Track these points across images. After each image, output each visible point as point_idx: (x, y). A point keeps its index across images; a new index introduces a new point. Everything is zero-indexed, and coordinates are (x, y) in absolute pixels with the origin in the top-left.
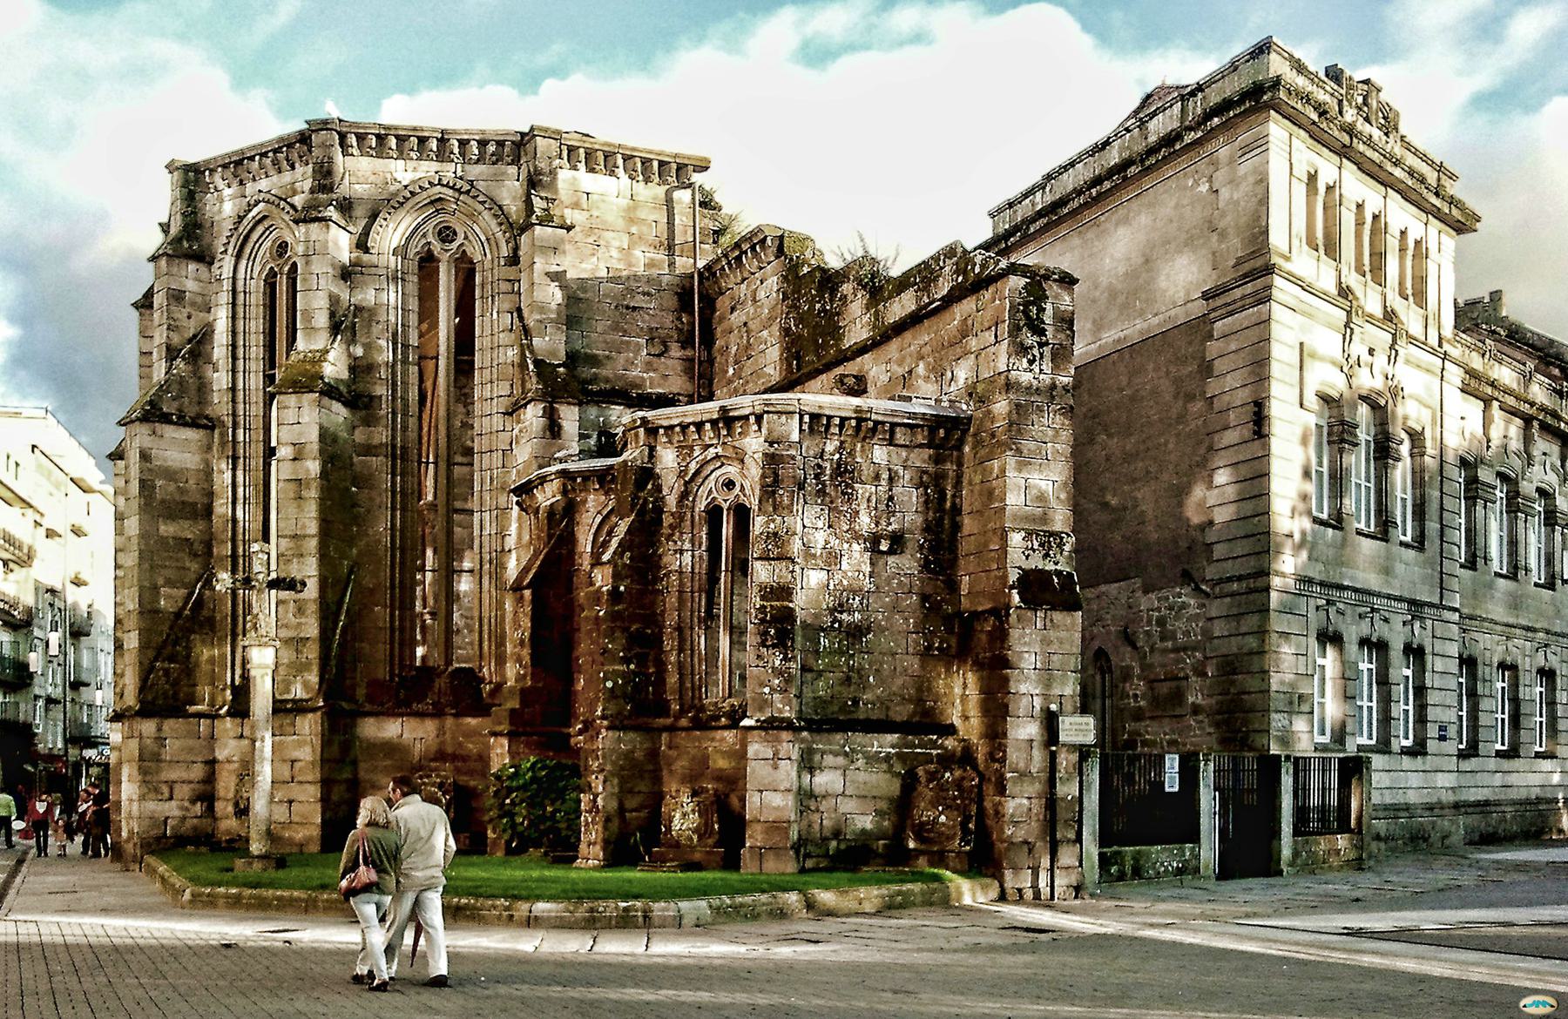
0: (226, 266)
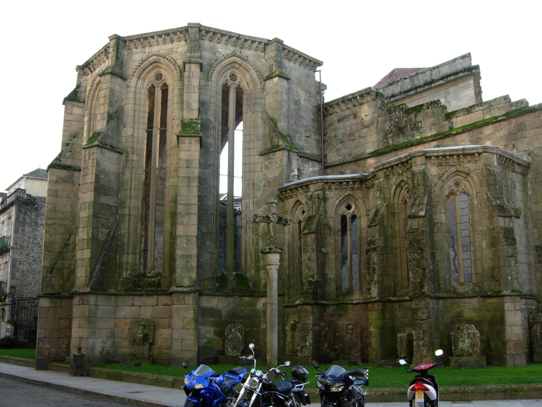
0: (133, 82)
